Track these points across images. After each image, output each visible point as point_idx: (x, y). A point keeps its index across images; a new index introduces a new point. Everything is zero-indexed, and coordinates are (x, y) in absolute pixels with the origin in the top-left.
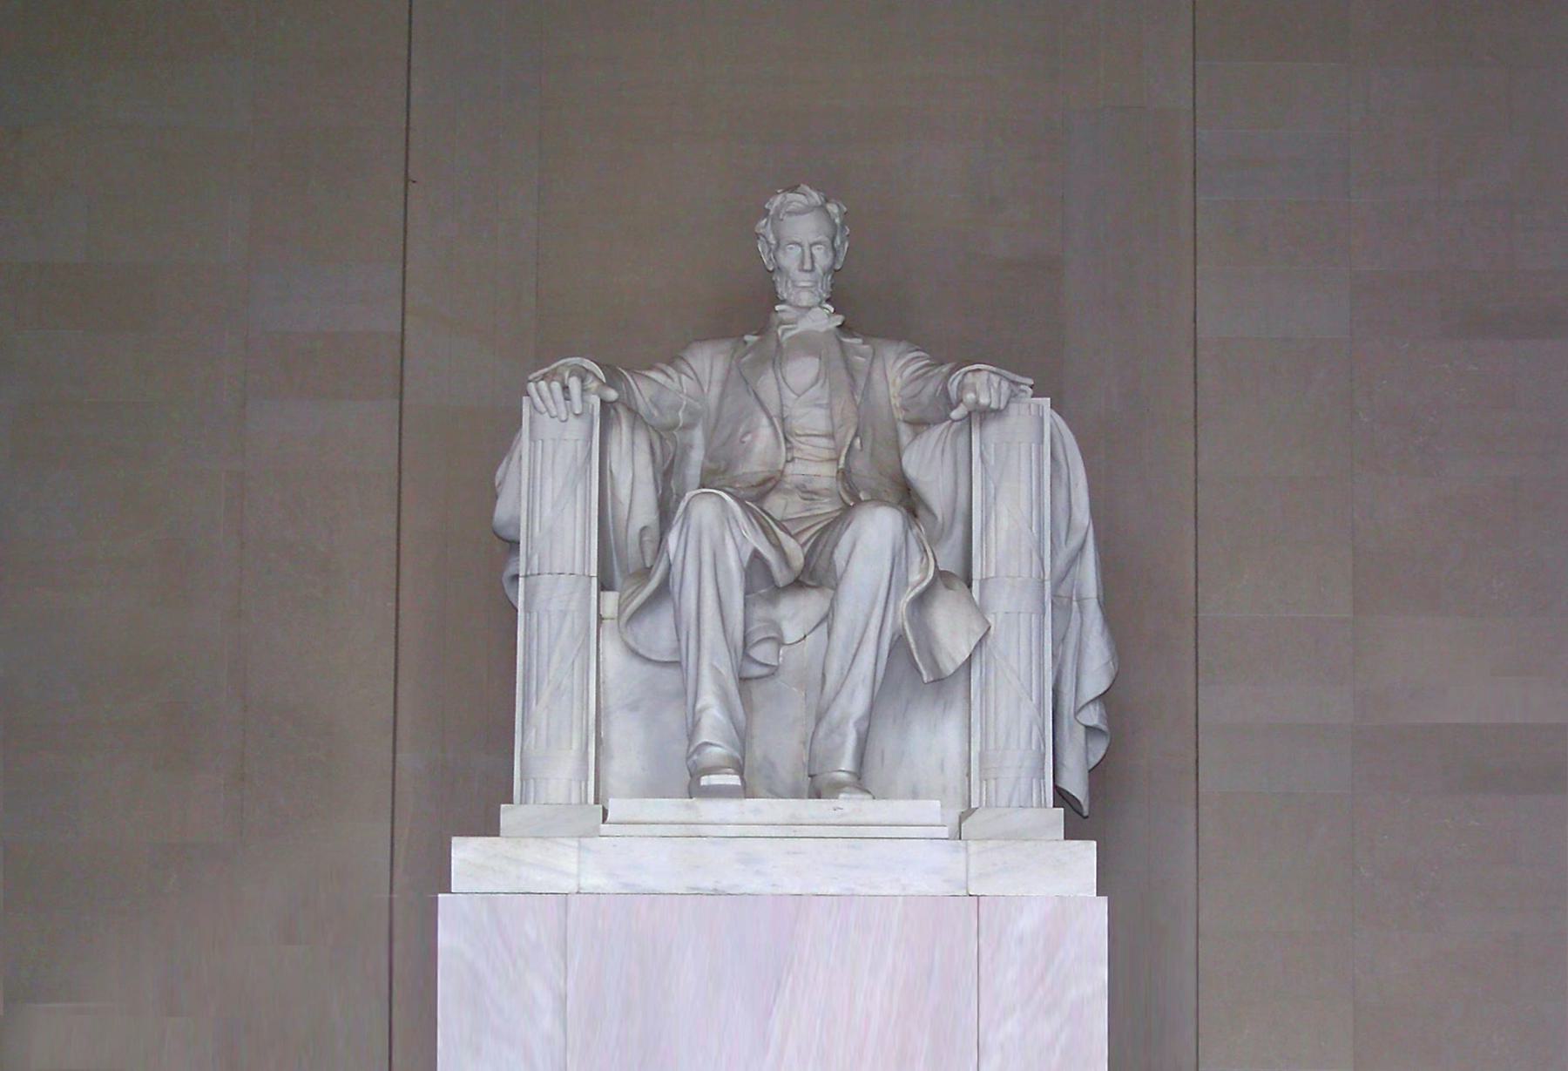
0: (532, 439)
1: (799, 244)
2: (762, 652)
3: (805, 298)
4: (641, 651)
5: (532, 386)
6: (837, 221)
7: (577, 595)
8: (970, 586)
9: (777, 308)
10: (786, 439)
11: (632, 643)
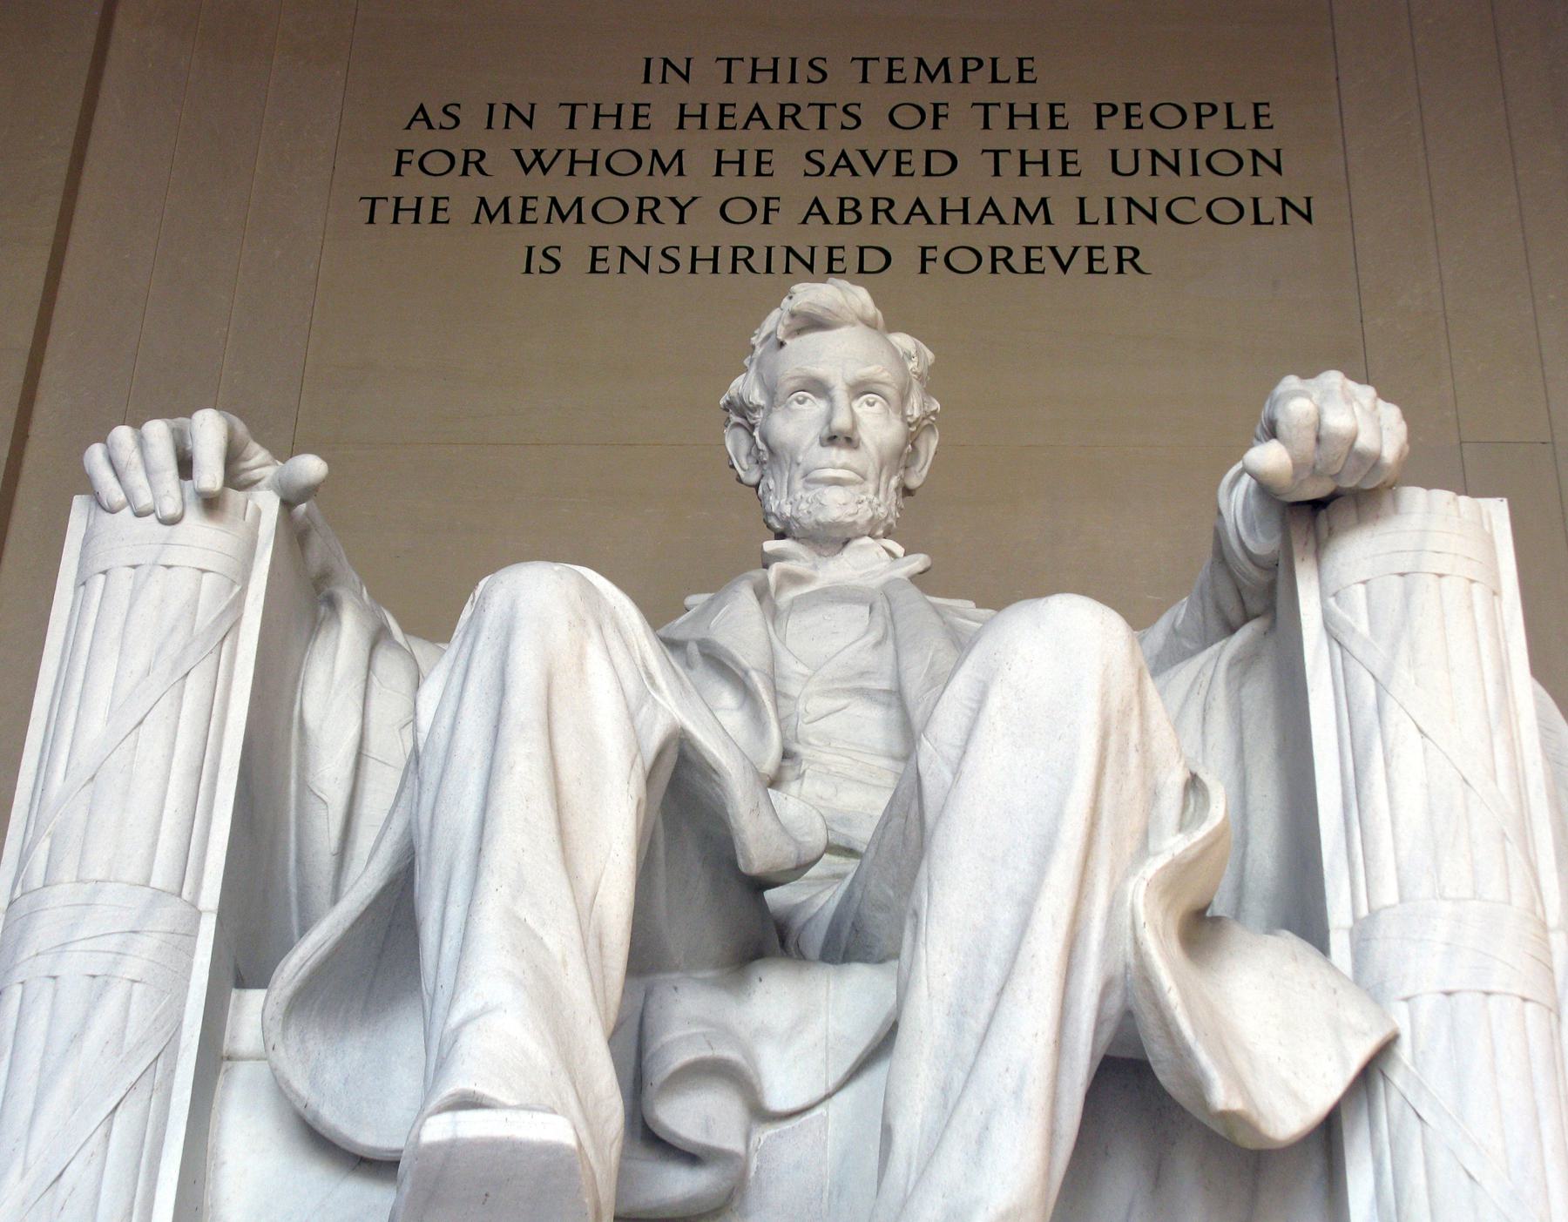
0: (82, 583)
1: (818, 388)
2: (691, 1115)
3: (836, 505)
4: (333, 1118)
5: (95, 456)
6: (911, 365)
7: (148, 945)
8: (1322, 946)
9: (770, 546)
10: (787, 755)
11: (300, 1084)
